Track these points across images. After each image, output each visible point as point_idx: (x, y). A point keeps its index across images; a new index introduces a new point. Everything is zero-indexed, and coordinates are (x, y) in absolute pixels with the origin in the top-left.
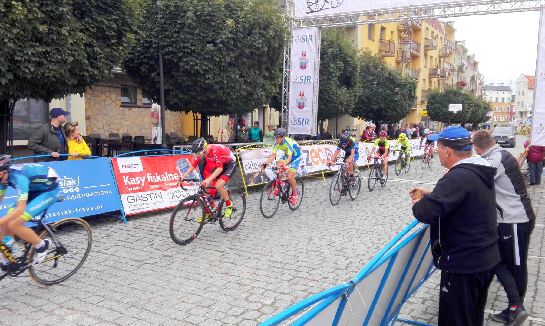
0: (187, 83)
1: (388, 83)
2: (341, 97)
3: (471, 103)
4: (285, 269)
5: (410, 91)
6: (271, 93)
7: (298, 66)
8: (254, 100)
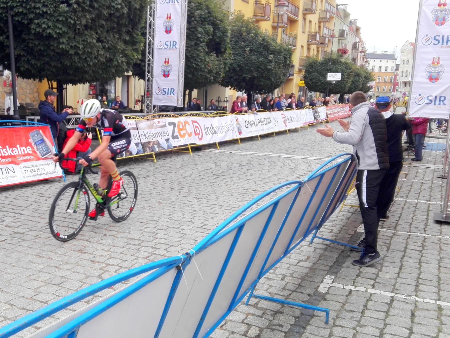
0: (39, 48)
1: (261, 50)
2: (211, 65)
3: (351, 72)
4: (142, 247)
5: (285, 58)
6: (132, 60)
7: (163, 30)
8: (114, 67)
